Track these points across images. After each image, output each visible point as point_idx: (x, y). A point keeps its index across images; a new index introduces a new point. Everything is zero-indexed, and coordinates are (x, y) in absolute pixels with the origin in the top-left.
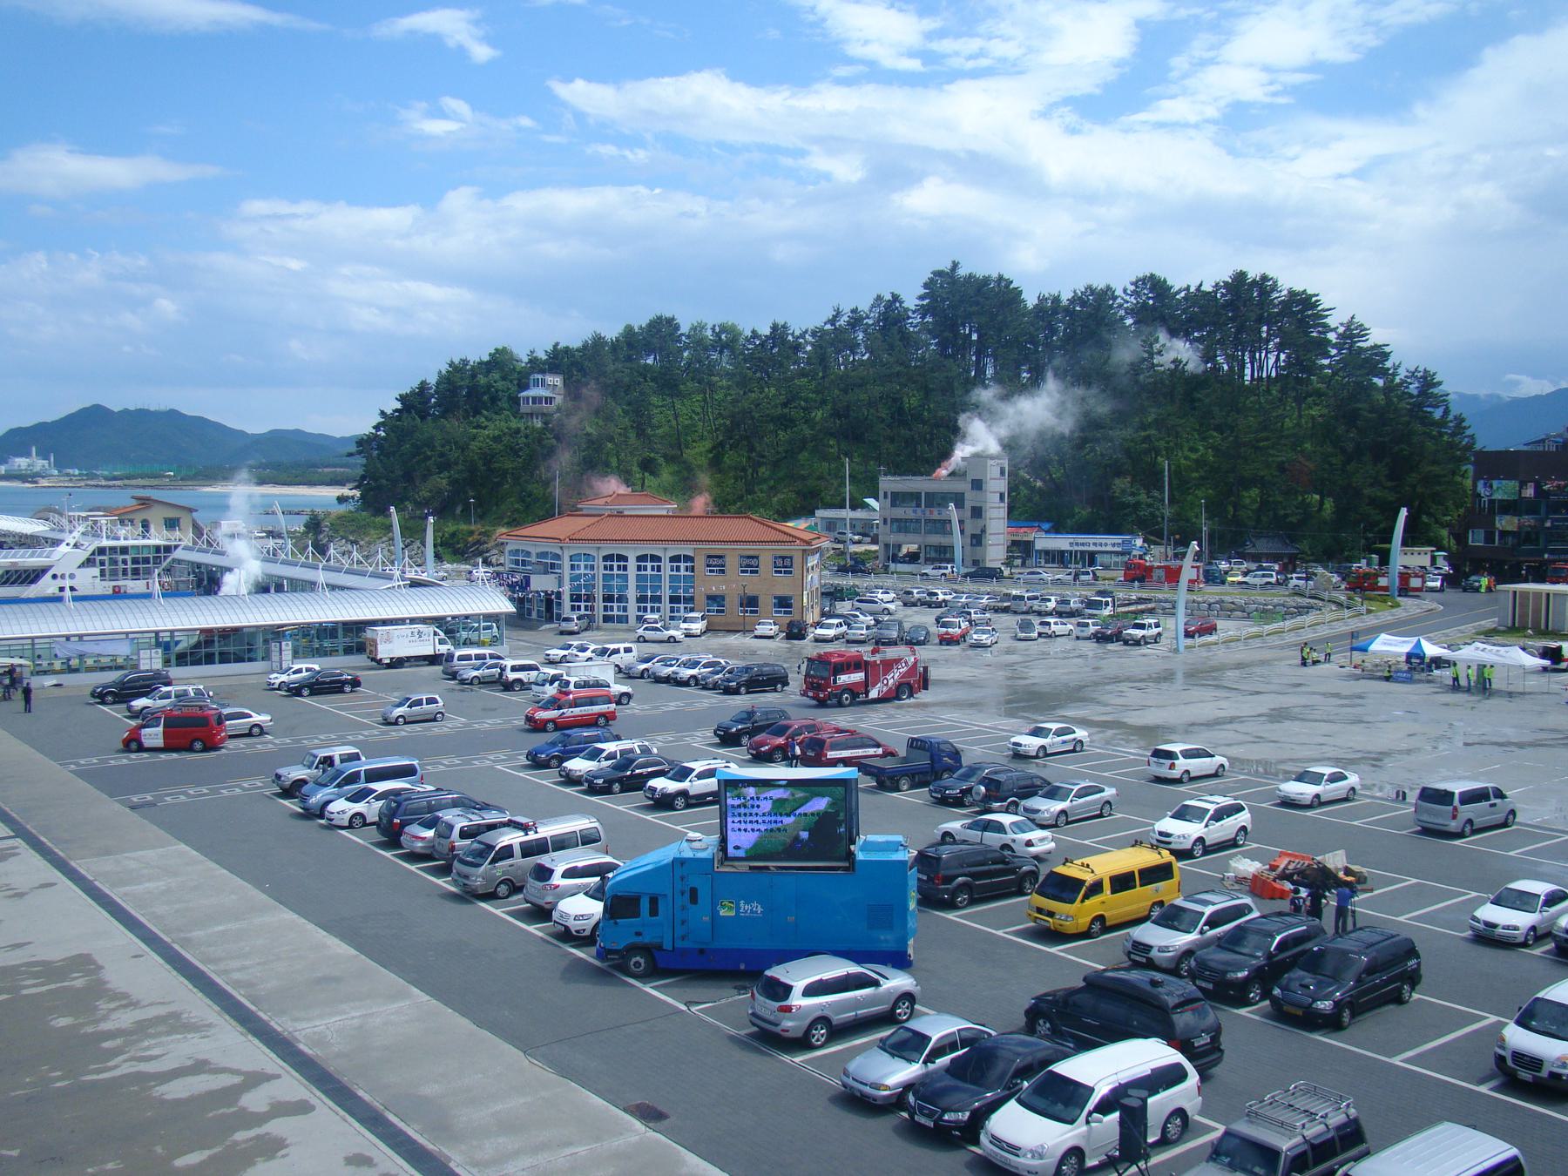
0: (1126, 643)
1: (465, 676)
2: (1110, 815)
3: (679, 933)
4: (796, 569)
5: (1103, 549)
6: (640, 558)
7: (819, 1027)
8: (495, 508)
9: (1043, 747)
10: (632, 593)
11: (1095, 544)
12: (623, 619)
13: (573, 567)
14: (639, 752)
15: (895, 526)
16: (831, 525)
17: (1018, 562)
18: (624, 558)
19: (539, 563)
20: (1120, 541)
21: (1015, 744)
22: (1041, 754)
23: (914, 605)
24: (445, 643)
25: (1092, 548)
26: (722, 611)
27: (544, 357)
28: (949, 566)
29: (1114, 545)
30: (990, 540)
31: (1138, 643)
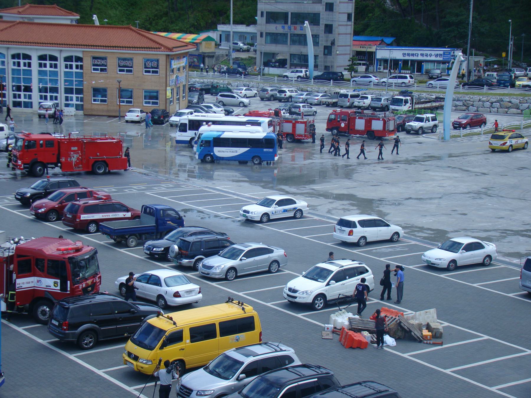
0: (408, 132)
2: (278, 271)
4: (162, 70)
5: (428, 58)
6: (42, 58)
9: (266, 214)
11: (422, 55)
12: (28, 105)
15: (269, 38)
16: (227, 36)
17: (362, 68)
18: (27, 57)
20: (442, 53)
21: (245, 211)
22: (265, 219)
23: (269, 99)
25: (420, 58)
26: (105, 101)
28: (304, 70)
29: (436, 56)
30: (337, 50)
31: (417, 132)
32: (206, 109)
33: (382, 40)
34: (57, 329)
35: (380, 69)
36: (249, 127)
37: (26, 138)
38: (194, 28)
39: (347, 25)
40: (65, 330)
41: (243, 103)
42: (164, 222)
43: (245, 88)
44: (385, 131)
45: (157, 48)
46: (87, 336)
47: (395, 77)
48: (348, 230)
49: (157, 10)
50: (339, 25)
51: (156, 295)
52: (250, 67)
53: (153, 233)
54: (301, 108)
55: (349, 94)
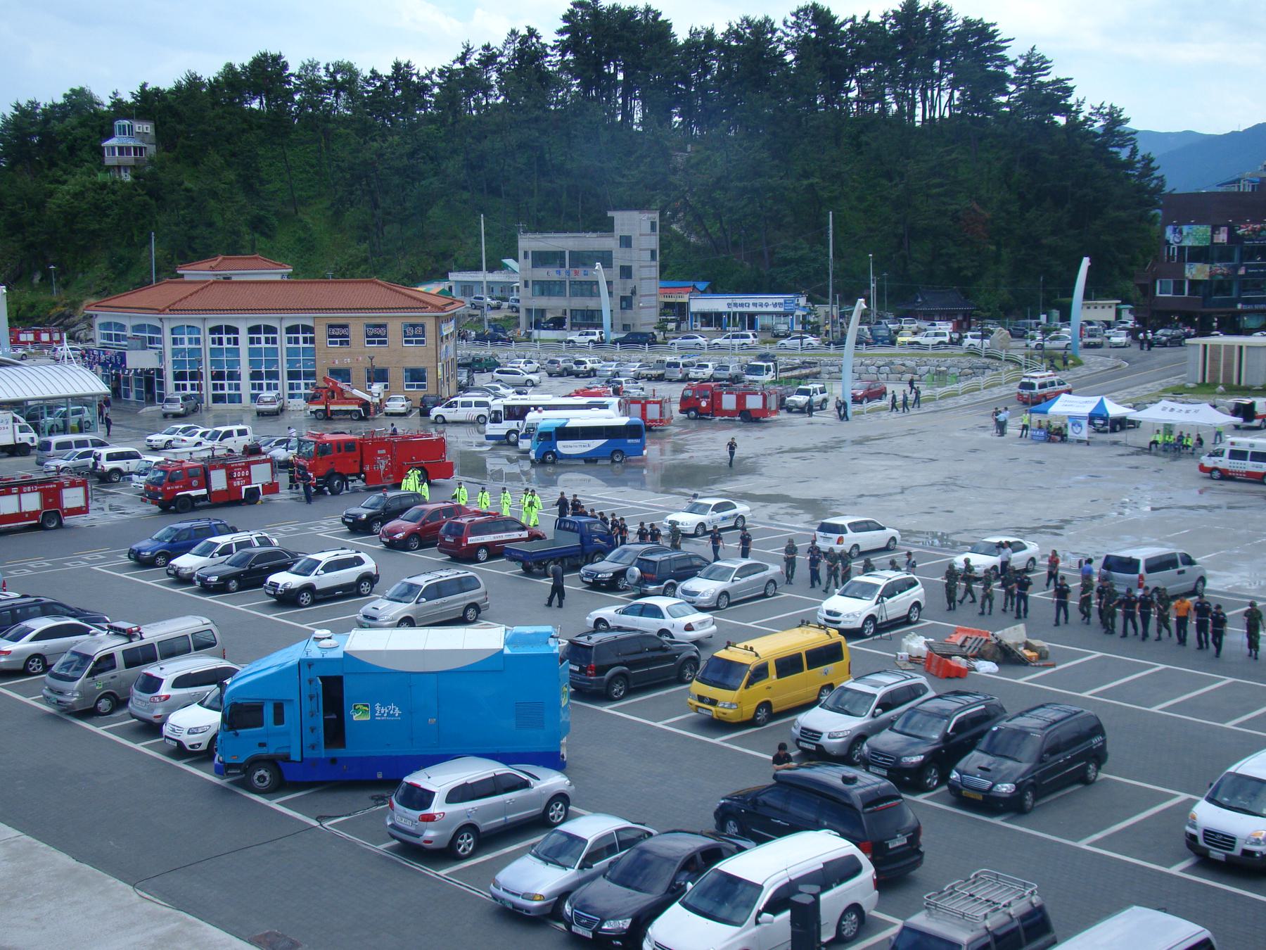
0: (789, 410)
2: (774, 595)
3: (307, 742)
5: (764, 309)
7: (465, 835)
10: (245, 370)
11: (755, 305)
12: (236, 399)
13: (175, 341)
14: (257, 544)
15: (537, 288)
16: (467, 288)
17: (672, 326)
19: (135, 338)
20: (782, 301)
22: (700, 533)
23: (560, 375)
25: (752, 309)
27: (130, 100)
28: (597, 332)
29: (775, 305)
33: (694, 287)
35: (696, 326)
36: (595, 411)
39: (651, 266)
40: (591, 675)
44: (765, 411)
47: (735, 337)
48: (836, 536)
50: (641, 267)
51: (657, 631)
54: (624, 385)
55: (681, 361)
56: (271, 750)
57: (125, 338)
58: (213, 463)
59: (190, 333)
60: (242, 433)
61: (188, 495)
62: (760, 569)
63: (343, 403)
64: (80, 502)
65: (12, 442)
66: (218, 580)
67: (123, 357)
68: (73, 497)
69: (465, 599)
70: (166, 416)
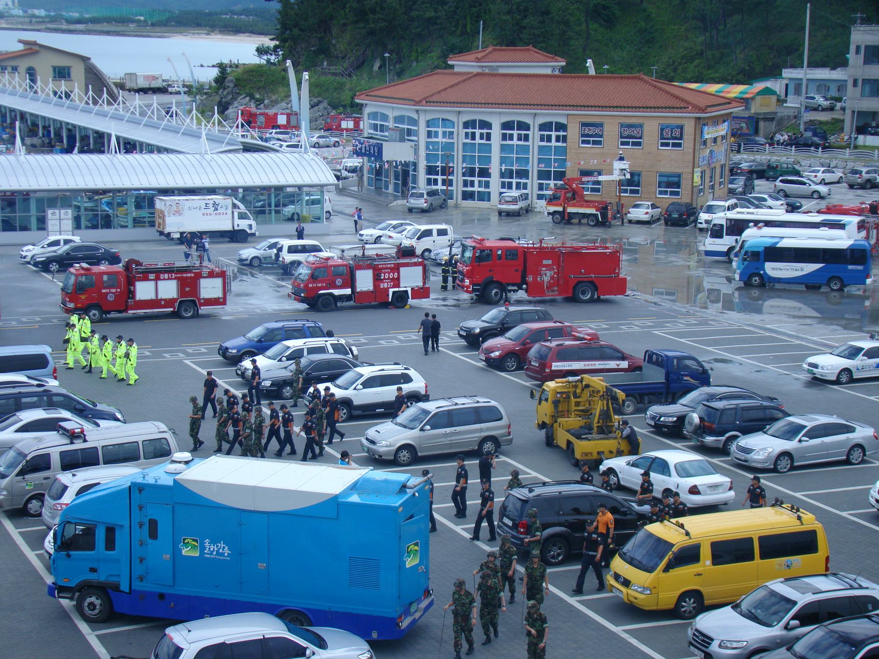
1: (244, 257)
2: (863, 462)
6: (507, 126)
8: (414, 64)
9: (847, 370)
12: (484, 197)
13: (429, 135)
14: (331, 350)
15: (867, 88)
16: (797, 86)
18: (486, 125)
21: (811, 365)
22: (844, 379)
23: (862, 187)
24: (248, 218)
32: (756, 203)
34: (510, 531)
36: (825, 232)
37: (477, 245)
38: (745, 75)
40: (522, 533)
41: (818, 192)
42: (679, 378)
43: (822, 169)
45: (681, 108)
46: (555, 545)
49: (686, 49)
51: (662, 489)
52: (833, 135)
53: (661, 394)
56: (101, 577)
57: (383, 128)
58: (364, 262)
59: (444, 126)
60: (443, 233)
61: (331, 294)
62: (846, 430)
63: (581, 206)
64: (218, 293)
65: (230, 228)
66: (272, 385)
67: (380, 148)
68: (210, 288)
69: (481, 430)
70: (410, 210)
